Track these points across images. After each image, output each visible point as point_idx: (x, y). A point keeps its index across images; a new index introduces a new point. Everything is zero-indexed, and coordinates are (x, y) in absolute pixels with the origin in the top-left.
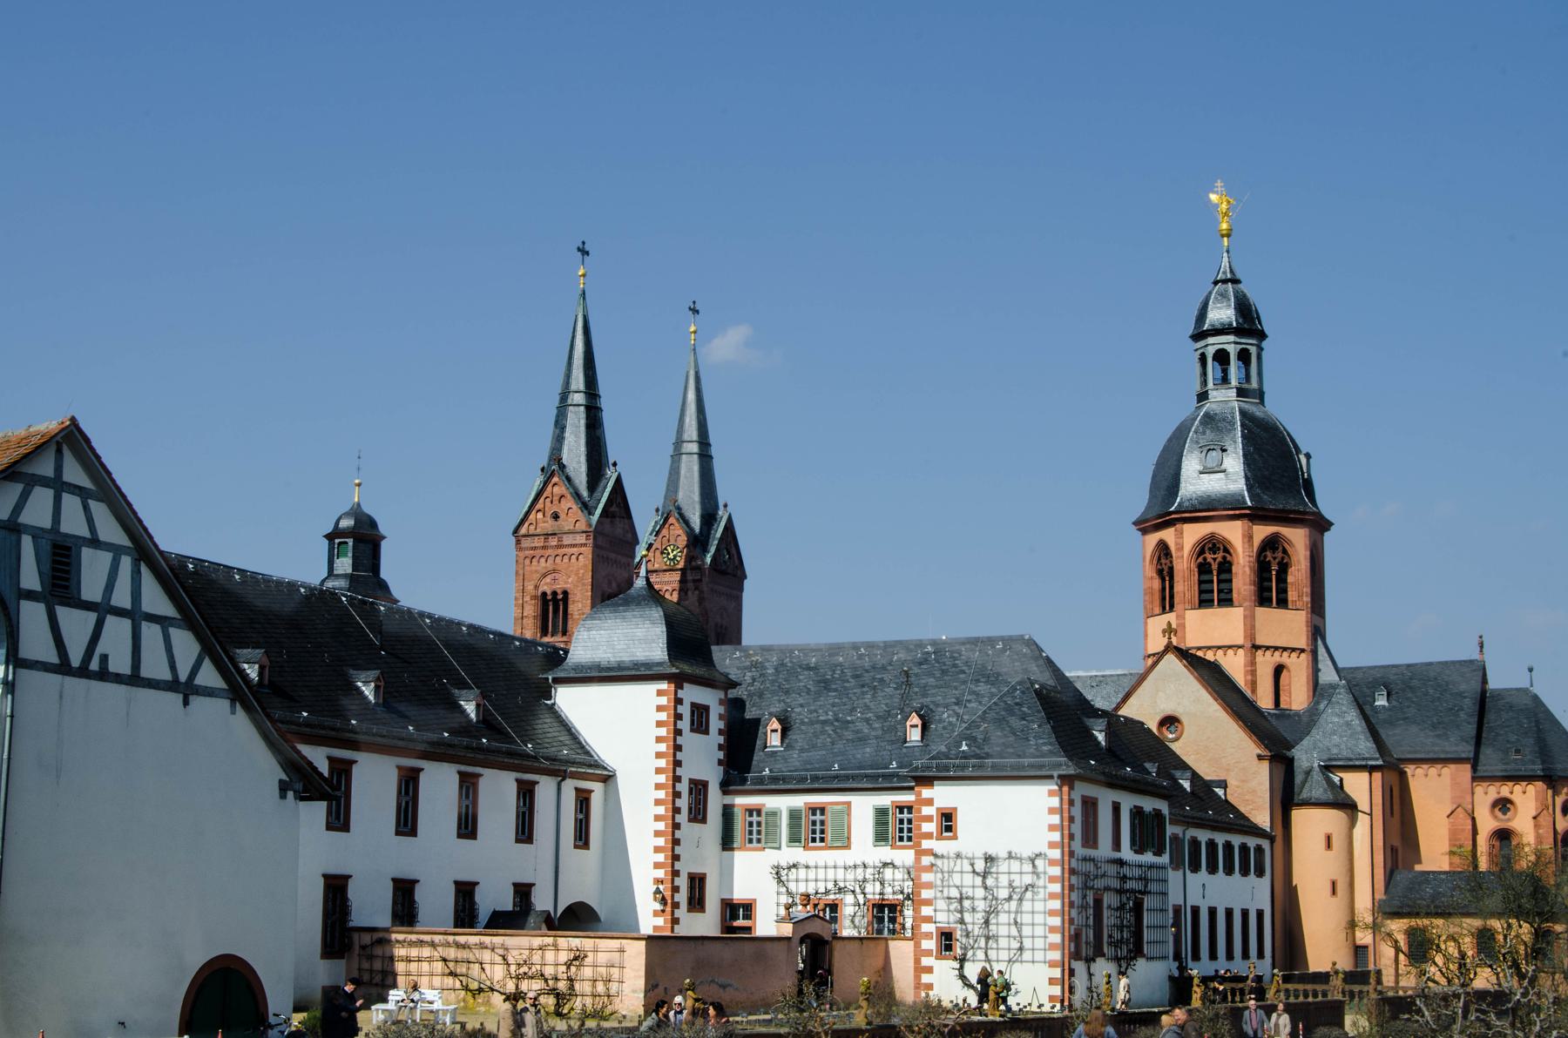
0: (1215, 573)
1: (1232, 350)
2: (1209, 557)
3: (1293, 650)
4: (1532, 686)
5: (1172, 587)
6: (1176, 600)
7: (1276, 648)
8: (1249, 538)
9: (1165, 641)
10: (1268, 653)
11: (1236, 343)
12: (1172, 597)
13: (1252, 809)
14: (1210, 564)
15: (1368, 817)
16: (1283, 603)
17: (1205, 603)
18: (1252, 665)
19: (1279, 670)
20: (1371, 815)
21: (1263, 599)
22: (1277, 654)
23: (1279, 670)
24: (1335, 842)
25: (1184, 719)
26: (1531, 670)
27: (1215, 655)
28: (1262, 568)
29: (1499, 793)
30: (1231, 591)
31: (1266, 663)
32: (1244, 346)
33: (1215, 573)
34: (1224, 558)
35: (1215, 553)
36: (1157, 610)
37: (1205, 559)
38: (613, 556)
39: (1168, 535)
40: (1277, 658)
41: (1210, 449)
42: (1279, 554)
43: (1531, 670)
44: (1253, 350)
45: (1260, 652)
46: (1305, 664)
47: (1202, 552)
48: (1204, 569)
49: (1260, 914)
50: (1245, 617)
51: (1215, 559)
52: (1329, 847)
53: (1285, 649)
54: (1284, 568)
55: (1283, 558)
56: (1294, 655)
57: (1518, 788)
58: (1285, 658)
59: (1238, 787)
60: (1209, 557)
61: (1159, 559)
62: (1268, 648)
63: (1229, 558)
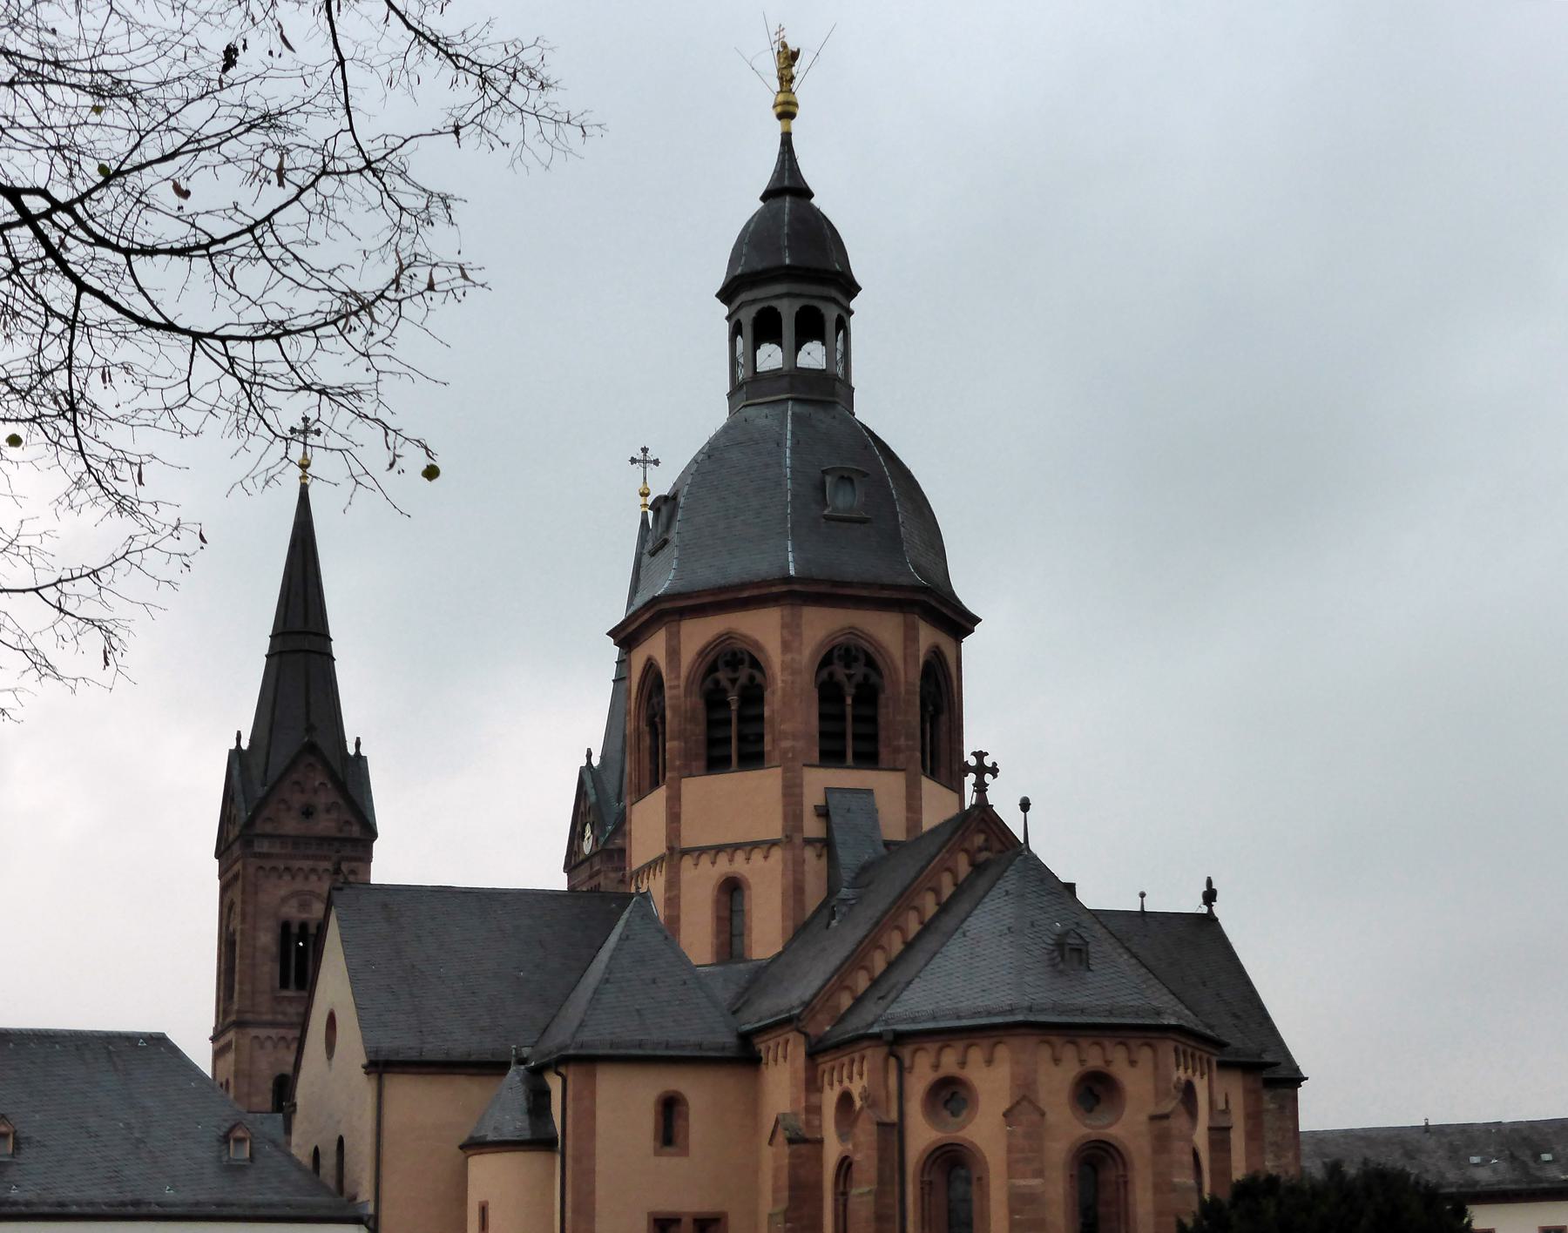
1: (788, 311)
3: (755, 845)
7: (719, 849)
8: (673, 653)
10: (705, 860)
11: (788, 295)
16: (753, 758)
18: (673, 884)
19: (732, 889)
21: (716, 763)
22: (723, 859)
23: (732, 889)
26: (1025, 805)
28: (714, 700)
31: (700, 882)
32: (765, 304)
38: (307, 864)
40: (724, 867)
42: (744, 673)
44: (788, 311)
45: (687, 862)
46: (780, 868)
50: (669, 799)
53: (737, 847)
54: (754, 695)
56: (757, 856)
58: (739, 866)
62: (702, 850)
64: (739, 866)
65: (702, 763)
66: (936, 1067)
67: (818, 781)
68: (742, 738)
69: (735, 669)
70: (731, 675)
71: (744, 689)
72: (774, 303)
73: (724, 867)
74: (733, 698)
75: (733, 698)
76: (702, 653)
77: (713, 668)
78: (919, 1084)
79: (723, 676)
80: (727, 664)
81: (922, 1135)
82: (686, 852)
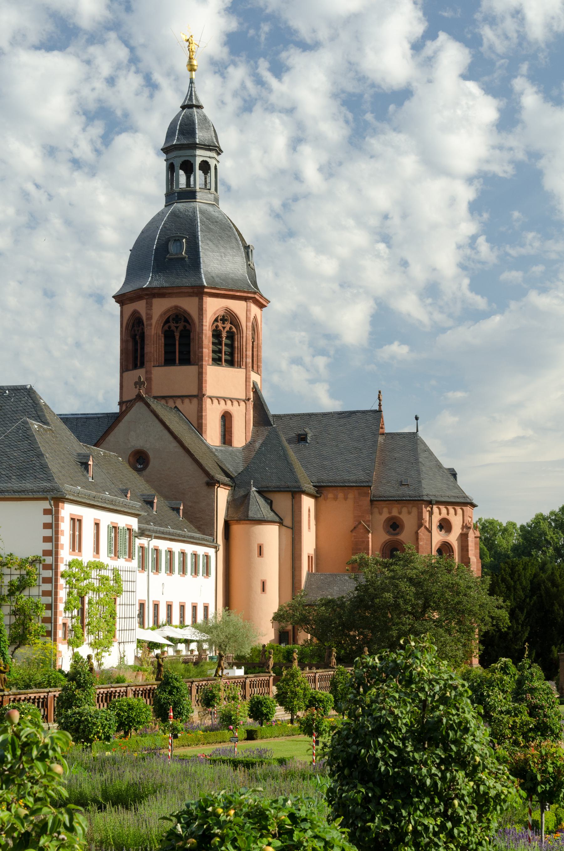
0: (177, 338)
2: (173, 325)
4: (417, 431)
5: (143, 348)
6: (146, 358)
9: (136, 392)
12: (143, 356)
13: (202, 525)
14: (173, 331)
15: (290, 531)
17: (169, 361)
20: (292, 529)
24: (265, 550)
25: (151, 455)
26: (417, 418)
27: (175, 403)
29: (390, 513)
30: (189, 352)
32: (205, 159)
33: (177, 338)
34: (185, 327)
35: (177, 322)
36: (131, 366)
37: (169, 327)
39: (140, 306)
41: (175, 240)
43: (417, 418)
47: (167, 321)
48: (168, 335)
49: (206, 608)
51: (177, 327)
52: (260, 555)
54: (231, 336)
55: (231, 328)
57: (405, 510)
59: (190, 507)
60: (173, 325)
61: (133, 326)
63: (188, 327)
64: (229, 407)
65: (211, 360)
66: (440, 514)
67: (254, 377)
68: (220, 351)
69: (223, 323)
70: (223, 325)
71: (227, 332)
72: (208, 160)
73: (222, 407)
74: (224, 335)
75: (224, 335)
76: (215, 314)
77: (216, 320)
78: (436, 518)
79: (220, 324)
80: (221, 320)
81: (438, 537)
82: (211, 398)
